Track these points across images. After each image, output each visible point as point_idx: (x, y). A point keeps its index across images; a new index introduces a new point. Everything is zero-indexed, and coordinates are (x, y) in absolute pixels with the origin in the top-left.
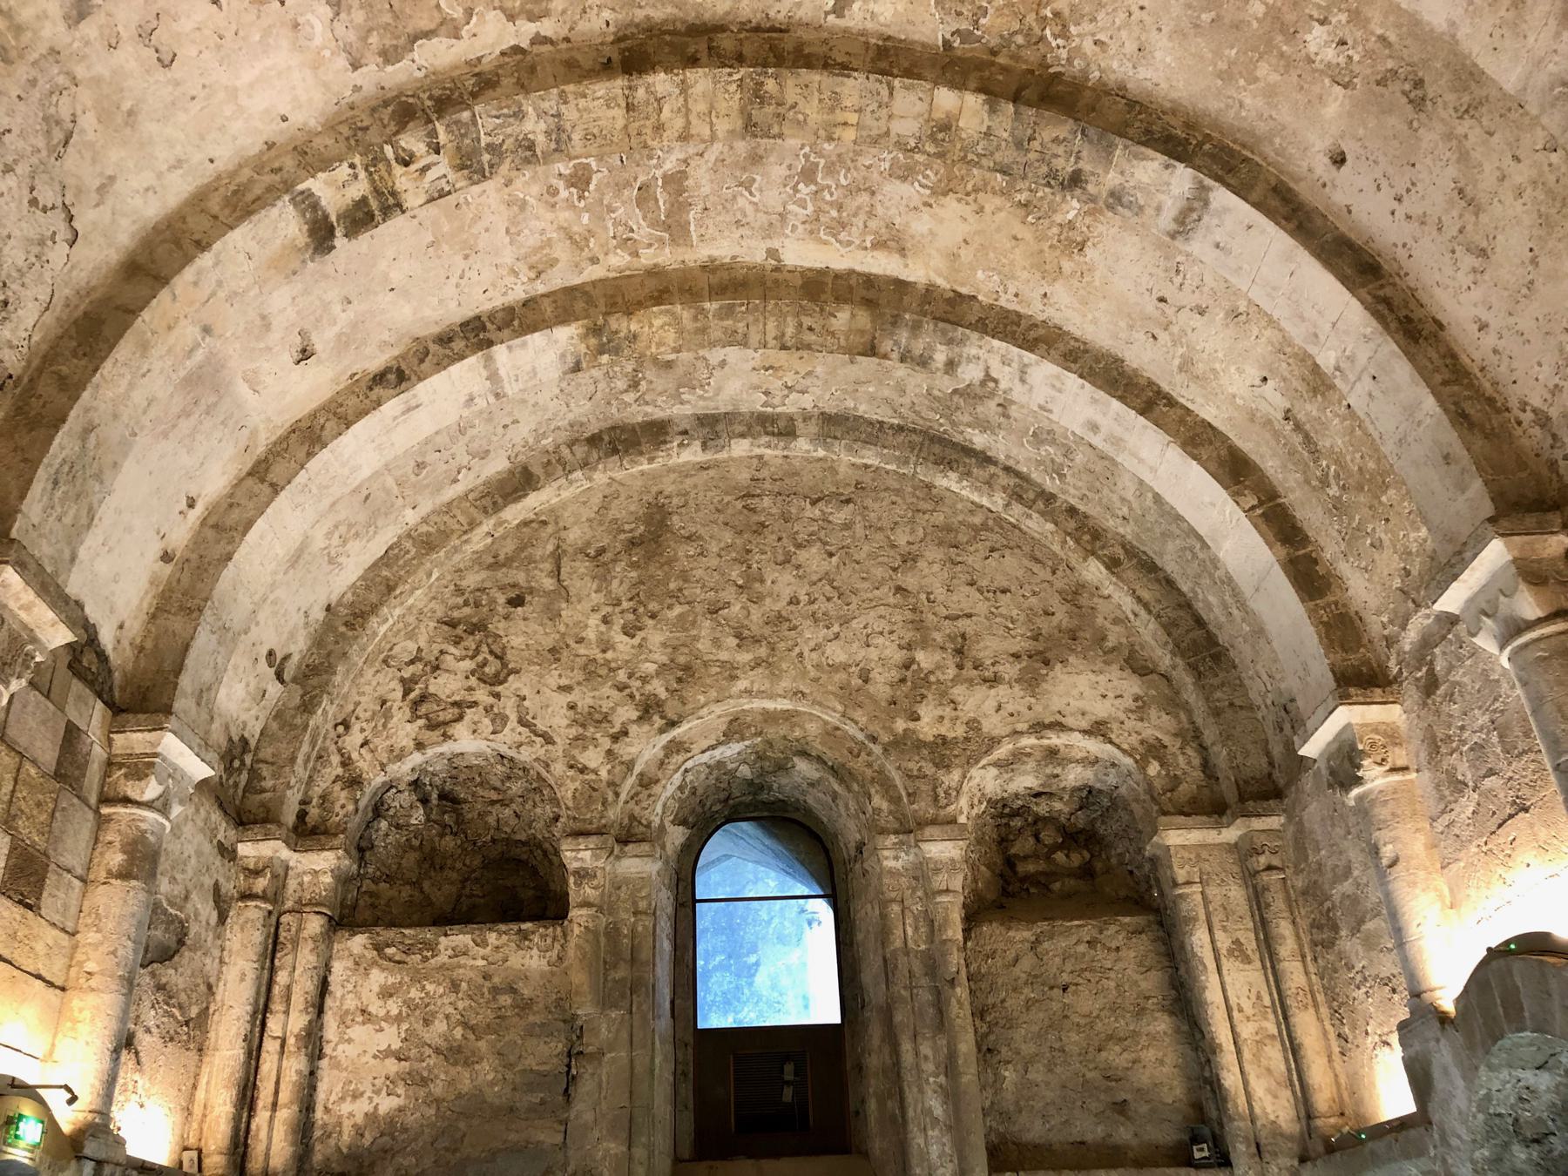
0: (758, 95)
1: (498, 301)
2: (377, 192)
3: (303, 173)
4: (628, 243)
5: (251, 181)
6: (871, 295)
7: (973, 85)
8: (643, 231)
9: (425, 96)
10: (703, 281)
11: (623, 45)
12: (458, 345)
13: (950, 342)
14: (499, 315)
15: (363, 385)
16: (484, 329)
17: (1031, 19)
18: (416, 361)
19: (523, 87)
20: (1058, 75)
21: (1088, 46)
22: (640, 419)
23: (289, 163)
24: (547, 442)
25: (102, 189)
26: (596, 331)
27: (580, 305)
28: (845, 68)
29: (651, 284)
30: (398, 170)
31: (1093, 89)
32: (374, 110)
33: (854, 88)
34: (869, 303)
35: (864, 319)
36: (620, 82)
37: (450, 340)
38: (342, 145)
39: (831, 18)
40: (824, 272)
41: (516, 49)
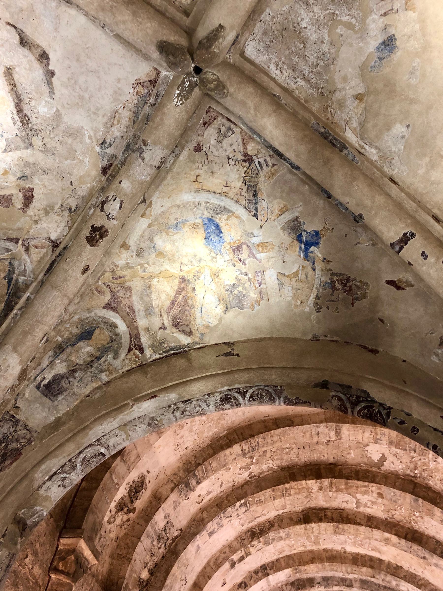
0: (337, 527)
1: (270, 560)
2: (246, 553)
3: (231, 554)
4: (304, 545)
5: (219, 556)
6: (372, 564)
7: (394, 532)
8: (308, 543)
9: (257, 529)
10: (324, 555)
11: (303, 513)
12: (260, 574)
13: (396, 580)
14: (270, 564)
15: (236, 587)
16: (266, 569)
17: (407, 518)
18: (249, 579)
19: (280, 527)
20: (416, 530)
21: (423, 527)
22: (306, 577)
23: (227, 550)
24: (280, 585)
25: (192, 570)
26: (296, 569)
27: (291, 562)
28: (360, 524)
29: (310, 555)
30: (251, 548)
31: (426, 536)
32: (246, 533)
33: (362, 529)
34: (372, 567)
35: (370, 570)
36: (303, 526)
37: (258, 573)
38: (239, 545)
39: (355, 509)
40: (358, 554)
41: (278, 515)
